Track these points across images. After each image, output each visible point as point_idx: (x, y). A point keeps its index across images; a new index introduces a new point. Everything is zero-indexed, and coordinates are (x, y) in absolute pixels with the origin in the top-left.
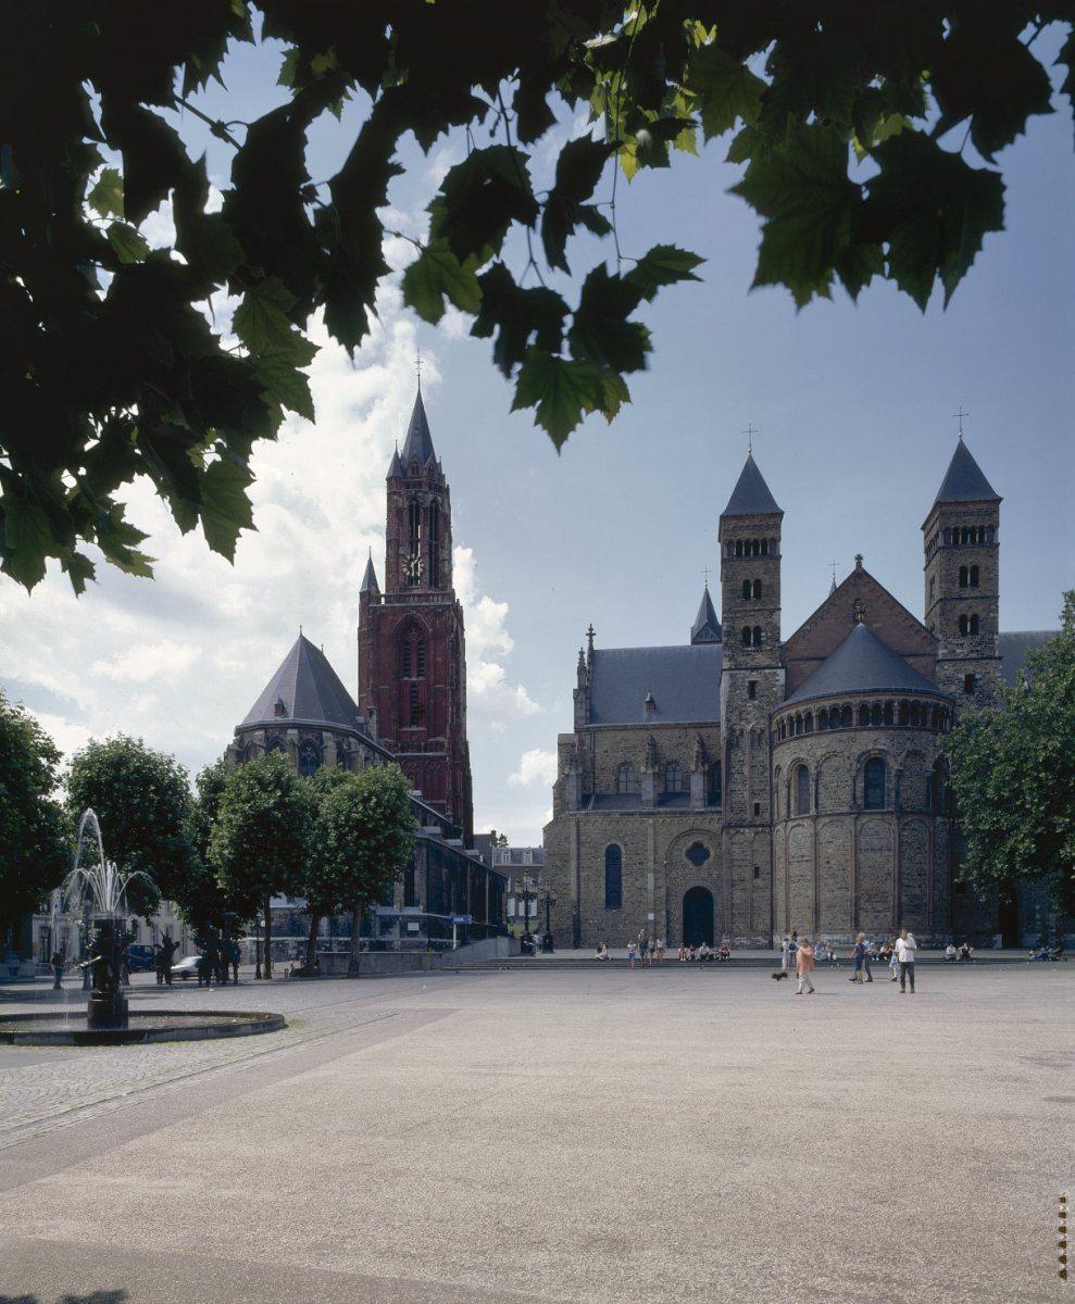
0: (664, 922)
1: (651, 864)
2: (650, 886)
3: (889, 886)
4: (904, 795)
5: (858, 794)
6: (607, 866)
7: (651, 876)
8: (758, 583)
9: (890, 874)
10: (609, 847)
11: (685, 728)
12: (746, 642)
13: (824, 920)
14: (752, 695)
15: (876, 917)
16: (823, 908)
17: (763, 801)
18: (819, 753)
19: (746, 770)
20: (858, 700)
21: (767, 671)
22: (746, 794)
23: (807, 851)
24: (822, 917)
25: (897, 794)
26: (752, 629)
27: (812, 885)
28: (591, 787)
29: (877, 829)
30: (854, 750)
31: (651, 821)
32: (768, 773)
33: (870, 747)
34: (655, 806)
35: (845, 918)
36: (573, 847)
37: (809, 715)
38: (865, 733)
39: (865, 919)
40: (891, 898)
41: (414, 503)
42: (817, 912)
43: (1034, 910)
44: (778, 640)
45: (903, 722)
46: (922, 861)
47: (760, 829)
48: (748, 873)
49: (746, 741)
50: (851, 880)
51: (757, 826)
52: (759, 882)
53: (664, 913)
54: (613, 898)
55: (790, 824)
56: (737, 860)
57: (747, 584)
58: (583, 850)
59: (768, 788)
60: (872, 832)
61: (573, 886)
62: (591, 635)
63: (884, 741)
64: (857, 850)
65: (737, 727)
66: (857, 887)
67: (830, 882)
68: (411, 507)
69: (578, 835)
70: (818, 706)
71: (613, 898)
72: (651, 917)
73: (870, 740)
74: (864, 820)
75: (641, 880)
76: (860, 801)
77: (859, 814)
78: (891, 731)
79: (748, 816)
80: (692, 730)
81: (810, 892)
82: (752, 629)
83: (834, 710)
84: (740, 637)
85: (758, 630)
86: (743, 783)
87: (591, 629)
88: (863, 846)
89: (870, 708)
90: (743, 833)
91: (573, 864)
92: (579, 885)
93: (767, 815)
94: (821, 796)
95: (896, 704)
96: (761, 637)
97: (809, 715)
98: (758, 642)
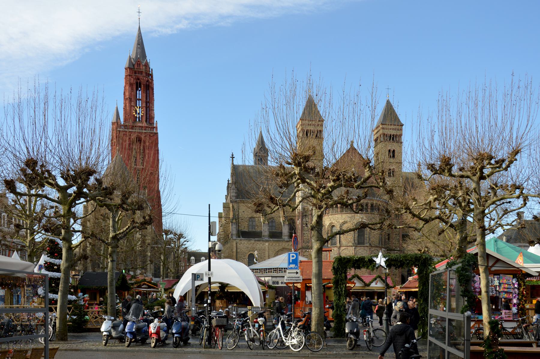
4: (371, 239)
5: (355, 239)
10: (250, 254)
25: (369, 240)
31: (267, 244)
41: (138, 81)
62: (233, 158)
68: (137, 83)
76: (356, 242)
77: (356, 246)
87: (233, 155)
90: (308, 251)
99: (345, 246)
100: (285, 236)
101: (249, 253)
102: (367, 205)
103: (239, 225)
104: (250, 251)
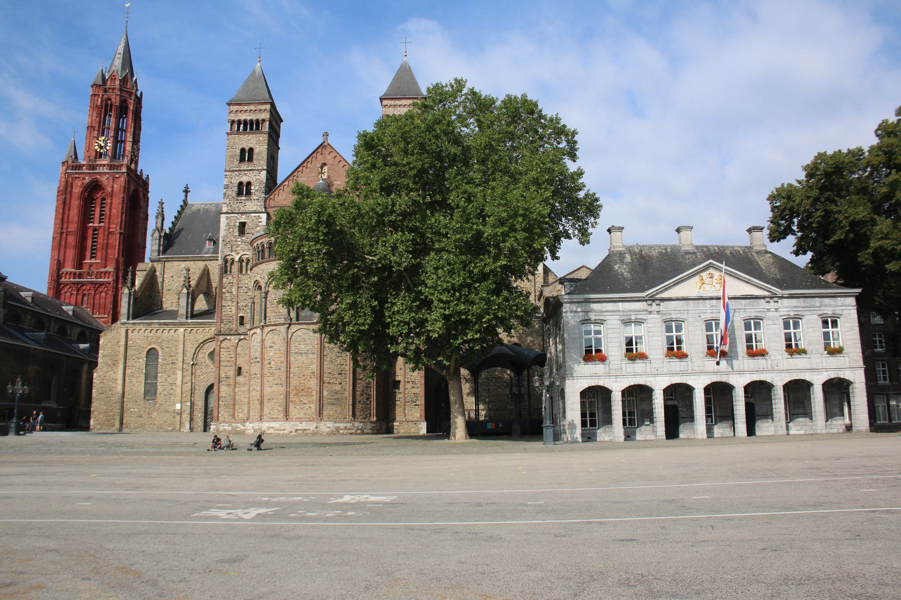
0: (189, 411)
1: (180, 364)
2: (179, 383)
3: (313, 384)
6: (146, 365)
7: (179, 373)
8: (251, 150)
12: (240, 193)
13: (266, 411)
16: (265, 401)
17: (247, 317)
19: (234, 290)
21: (252, 215)
22: (233, 308)
24: (265, 408)
26: (245, 184)
29: (304, 336)
31: (182, 330)
34: (187, 318)
35: (279, 409)
36: (122, 349)
39: (294, 411)
40: (314, 393)
42: (262, 403)
46: (343, 362)
47: (242, 337)
48: (232, 373)
49: (235, 268)
50: (284, 378)
51: (239, 334)
52: (240, 379)
53: (189, 404)
54: (150, 391)
56: (224, 361)
57: (243, 150)
58: (129, 352)
60: (299, 339)
61: (120, 382)
64: (288, 353)
65: (229, 258)
66: (288, 384)
67: (271, 379)
69: (127, 341)
71: (150, 391)
72: (178, 406)
74: (294, 328)
75: (173, 376)
79: (234, 326)
81: (259, 388)
82: (245, 184)
84: (236, 189)
85: (249, 184)
88: (293, 349)
91: (121, 366)
92: (124, 380)
96: (251, 189)
97: (263, 246)
98: (249, 193)
101: (149, 347)
104: (150, 344)
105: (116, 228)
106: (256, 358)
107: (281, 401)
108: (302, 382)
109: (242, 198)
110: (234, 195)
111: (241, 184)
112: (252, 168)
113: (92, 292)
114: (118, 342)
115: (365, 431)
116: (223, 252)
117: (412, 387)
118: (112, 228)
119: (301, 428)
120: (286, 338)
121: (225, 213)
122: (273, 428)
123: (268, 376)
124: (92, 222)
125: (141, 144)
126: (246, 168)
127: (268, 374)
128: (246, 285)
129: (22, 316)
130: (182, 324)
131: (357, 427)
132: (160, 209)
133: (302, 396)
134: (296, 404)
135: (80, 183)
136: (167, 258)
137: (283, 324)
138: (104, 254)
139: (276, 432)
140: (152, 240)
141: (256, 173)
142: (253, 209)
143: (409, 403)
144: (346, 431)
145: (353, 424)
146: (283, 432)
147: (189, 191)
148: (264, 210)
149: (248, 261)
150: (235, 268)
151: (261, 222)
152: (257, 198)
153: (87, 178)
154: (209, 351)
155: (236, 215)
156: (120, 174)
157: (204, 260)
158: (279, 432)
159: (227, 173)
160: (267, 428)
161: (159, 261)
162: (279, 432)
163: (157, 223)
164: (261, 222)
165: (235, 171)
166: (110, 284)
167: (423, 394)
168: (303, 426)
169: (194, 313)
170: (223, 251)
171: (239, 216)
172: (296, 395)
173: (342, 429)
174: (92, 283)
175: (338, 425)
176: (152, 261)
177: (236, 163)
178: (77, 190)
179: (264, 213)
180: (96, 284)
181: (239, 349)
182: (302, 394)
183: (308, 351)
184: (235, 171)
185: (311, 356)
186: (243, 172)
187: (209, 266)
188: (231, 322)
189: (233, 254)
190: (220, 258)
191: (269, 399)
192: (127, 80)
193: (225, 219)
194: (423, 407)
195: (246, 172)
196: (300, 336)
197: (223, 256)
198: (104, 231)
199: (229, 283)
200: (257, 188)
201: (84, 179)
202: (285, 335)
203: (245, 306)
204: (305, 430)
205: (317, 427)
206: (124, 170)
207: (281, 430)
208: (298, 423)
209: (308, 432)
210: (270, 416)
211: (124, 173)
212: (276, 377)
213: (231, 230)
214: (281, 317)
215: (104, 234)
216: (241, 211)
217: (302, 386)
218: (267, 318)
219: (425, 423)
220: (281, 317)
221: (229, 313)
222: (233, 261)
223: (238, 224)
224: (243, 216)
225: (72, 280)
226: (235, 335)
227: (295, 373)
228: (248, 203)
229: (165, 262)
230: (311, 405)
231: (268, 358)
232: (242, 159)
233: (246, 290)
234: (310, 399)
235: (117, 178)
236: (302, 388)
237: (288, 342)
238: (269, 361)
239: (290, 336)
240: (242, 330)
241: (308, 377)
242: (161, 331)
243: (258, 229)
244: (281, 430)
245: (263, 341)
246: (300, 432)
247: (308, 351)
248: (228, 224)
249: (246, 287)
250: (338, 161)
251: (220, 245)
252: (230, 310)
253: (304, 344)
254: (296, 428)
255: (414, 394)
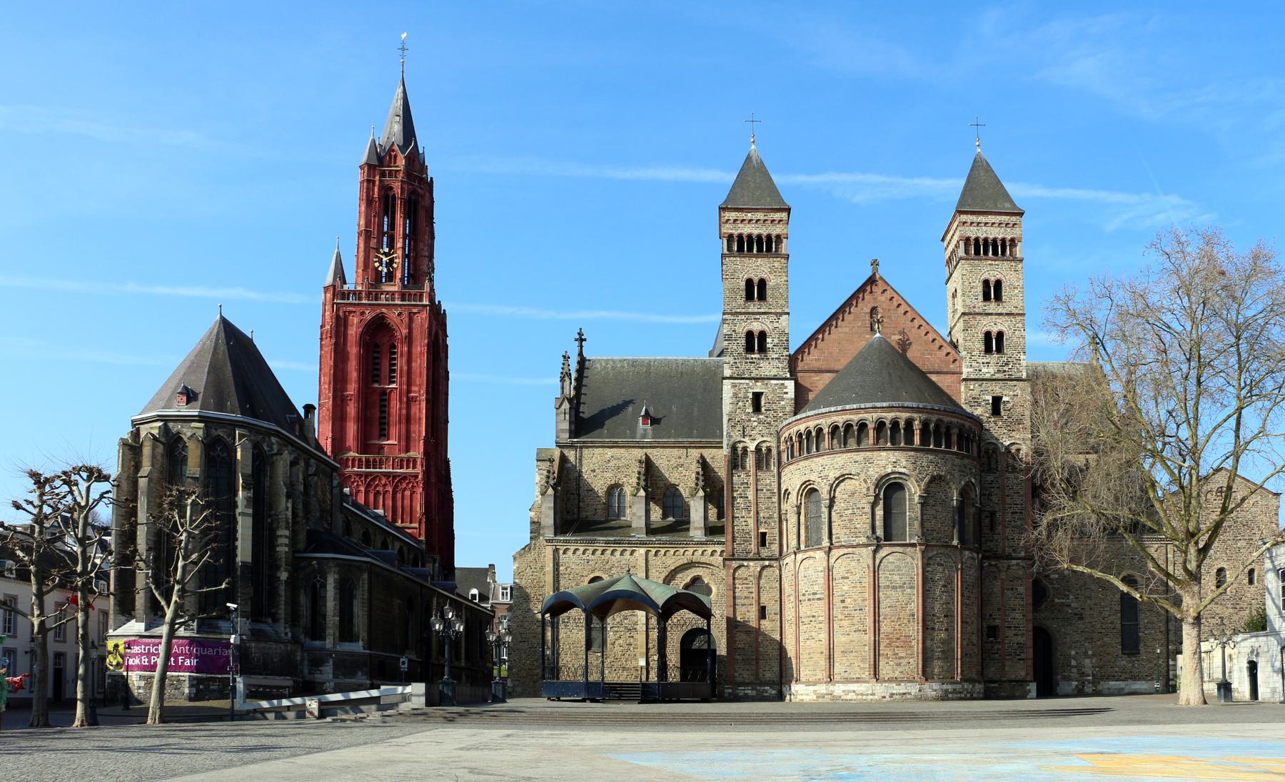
8: (762, 283)
9: (913, 615)
11: (686, 448)
12: (749, 348)
13: (838, 668)
14: (757, 408)
15: (899, 665)
17: (772, 533)
18: (833, 475)
19: (751, 494)
20: (875, 416)
21: (772, 382)
22: (751, 522)
23: (820, 587)
24: (837, 665)
26: (756, 334)
27: (825, 626)
28: (576, 510)
30: (871, 472)
31: (642, 551)
32: (775, 499)
33: (889, 471)
37: (820, 431)
38: (884, 454)
39: (886, 669)
40: (914, 643)
42: (830, 658)
43: (1070, 656)
44: (787, 348)
45: (924, 441)
47: (767, 563)
49: (750, 461)
50: (869, 622)
55: (800, 557)
59: (776, 515)
60: (891, 567)
63: (904, 463)
67: (845, 623)
70: (830, 421)
73: (888, 461)
76: (880, 532)
78: (912, 453)
79: (753, 547)
80: (694, 451)
82: (756, 334)
83: (848, 427)
85: (763, 335)
86: (748, 509)
88: (883, 582)
89: (888, 425)
93: (775, 547)
94: (834, 525)
95: (916, 423)
97: (820, 431)
98: (763, 349)
99: (849, 547)
100: (696, 528)
101: (592, 576)
102: (909, 423)
103: (581, 504)
104: (593, 571)
105: (420, 391)
106: (816, 594)
107: (864, 654)
108: (897, 627)
109: (753, 356)
110: (741, 350)
111: (750, 335)
112: (767, 310)
113: (390, 489)
114: (542, 568)
115: (975, 695)
116: (730, 436)
117: (1015, 635)
118: (415, 392)
119: (898, 691)
120: (871, 566)
121: (731, 378)
122: (854, 691)
123: (841, 620)
124: (377, 382)
125: (435, 261)
126: (756, 310)
127: (840, 617)
128: (768, 487)
129: (352, 524)
130: (642, 543)
131: (967, 689)
132: (566, 366)
133: (898, 647)
134: (888, 658)
135: (356, 320)
136: (584, 442)
137: (867, 546)
138: (403, 431)
139: (860, 697)
140: (557, 414)
141: (773, 317)
142: (772, 373)
143: (1010, 657)
144: (955, 695)
145: (963, 686)
146: (871, 697)
147: (585, 340)
148: (788, 375)
149: (769, 450)
150: (750, 461)
151: (787, 393)
152: (777, 356)
153: (367, 312)
154: (684, 583)
155: (747, 381)
156: (421, 308)
157: (643, 448)
158: (864, 697)
159: (726, 317)
160: (844, 691)
161: (570, 446)
162: (864, 697)
163: (563, 388)
164: (787, 393)
165: (741, 313)
166: (416, 477)
167: (1030, 643)
168: (901, 689)
169: (652, 527)
170: (729, 434)
171: (751, 383)
172: (889, 645)
173: (950, 693)
174: (387, 475)
175: (945, 687)
176: (560, 447)
177: (742, 301)
178: (354, 331)
179: (791, 379)
180: (394, 477)
181: (762, 581)
182: (897, 644)
183: (905, 583)
184: (741, 313)
185: (909, 590)
186: (753, 317)
187: (651, 457)
188: (746, 541)
189: (746, 439)
190: (725, 445)
191: (842, 652)
192: (416, 164)
193: (730, 387)
194: (1030, 663)
195: (758, 317)
196: (894, 563)
197: (731, 443)
198: (400, 397)
199: (742, 484)
200: (776, 341)
201: (363, 314)
202: (871, 562)
203: (769, 518)
204: (904, 694)
205: (920, 691)
206: (426, 302)
207: (867, 695)
208: (894, 685)
209: (909, 696)
210: (846, 675)
211: (426, 306)
212: (856, 620)
213: (740, 403)
214: (859, 535)
215: (401, 401)
216: (753, 375)
217: (897, 633)
218: (834, 537)
219: (1035, 684)
220: (859, 535)
221: (744, 528)
222: (745, 449)
223: (750, 396)
224: (759, 384)
225: (356, 469)
226: (757, 560)
227: (887, 615)
228: (763, 364)
229: (581, 448)
230: (911, 660)
231: (840, 593)
232: (749, 297)
233: (768, 494)
234: (908, 652)
235: (415, 313)
236: (898, 636)
237: (875, 571)
238: (841, 598)
239: (877, 562)
240: (765, 552)
241: (905, 621)
242: (599, 552)
243: (782, 403)
244: (867, 695)
245: (829, 569)
246: (898, 697)
247: (905, 583)
248: (735, 395)
249: (768, 490)
250: (896, 304)
251: (725, 426)
252: (743, 523)
253: (899, 574)
254: (890, 691)
255: (1018, 644)
